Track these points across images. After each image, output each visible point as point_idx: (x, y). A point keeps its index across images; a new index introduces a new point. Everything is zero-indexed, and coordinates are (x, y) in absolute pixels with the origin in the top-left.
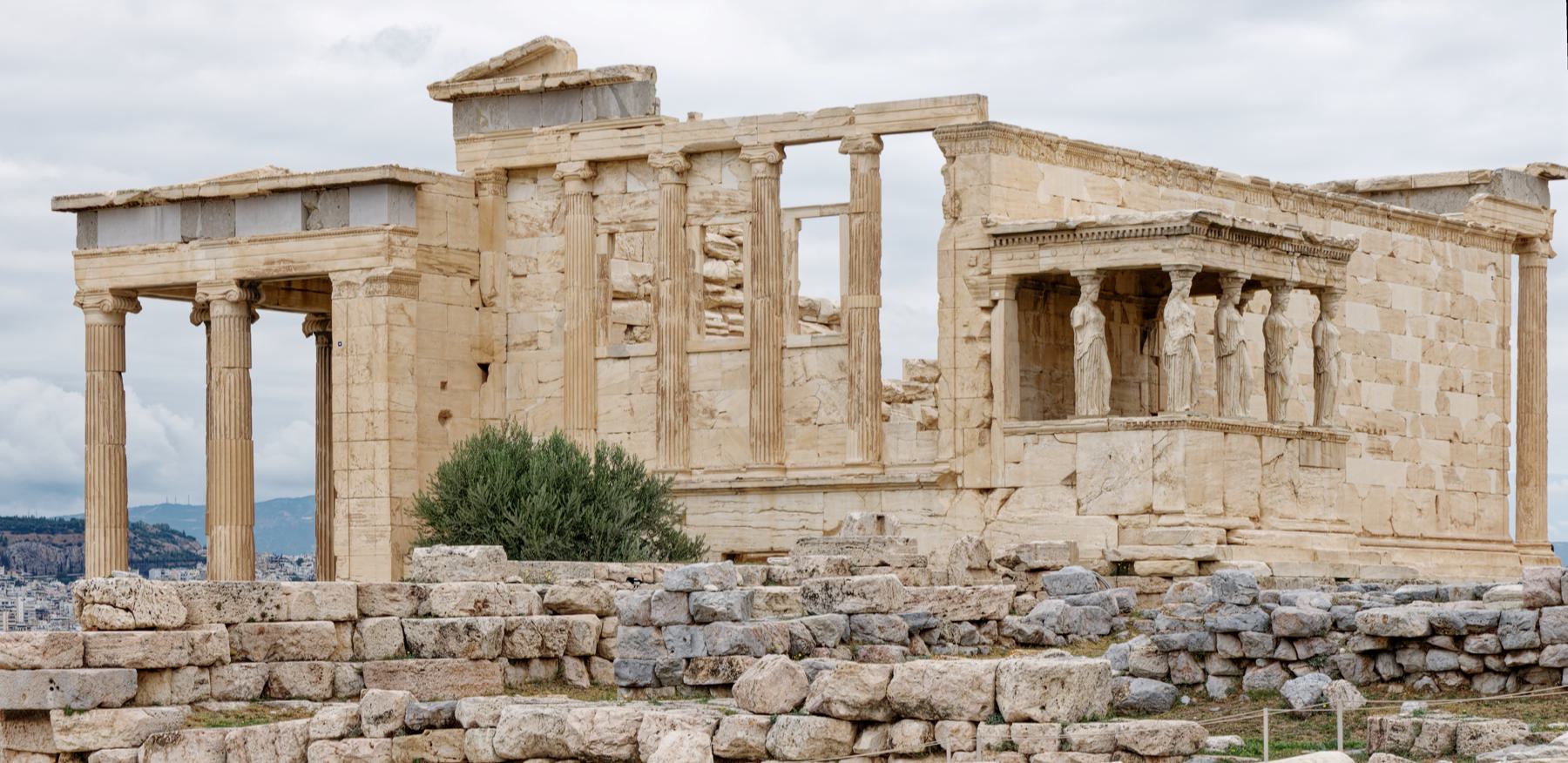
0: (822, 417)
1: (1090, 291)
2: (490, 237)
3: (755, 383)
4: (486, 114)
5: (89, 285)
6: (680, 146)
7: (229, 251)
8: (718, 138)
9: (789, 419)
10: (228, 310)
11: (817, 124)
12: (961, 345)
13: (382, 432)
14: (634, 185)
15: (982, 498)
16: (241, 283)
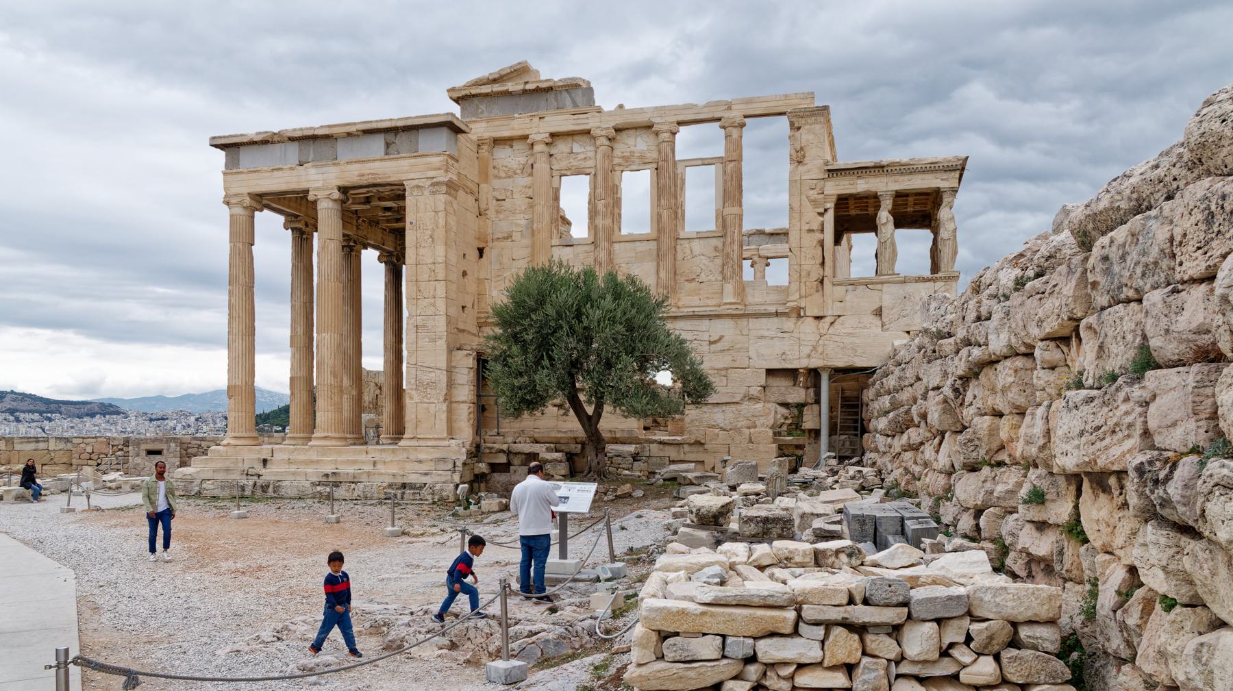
0: (703, 277)
1: (887, 203)
2: (484, 175)
3: (659, 256)
4: (483, 107)
5: (233, 191)
6: (613, 124)
7: (333, 169)
8: (639, 119)
9: (681, 279)
10: (331, 204)
11: (707, 110)
12: (804, 235)
13: (441, 275)
14: (577, 148)
15: (816, 322)
16: (340, 189)
